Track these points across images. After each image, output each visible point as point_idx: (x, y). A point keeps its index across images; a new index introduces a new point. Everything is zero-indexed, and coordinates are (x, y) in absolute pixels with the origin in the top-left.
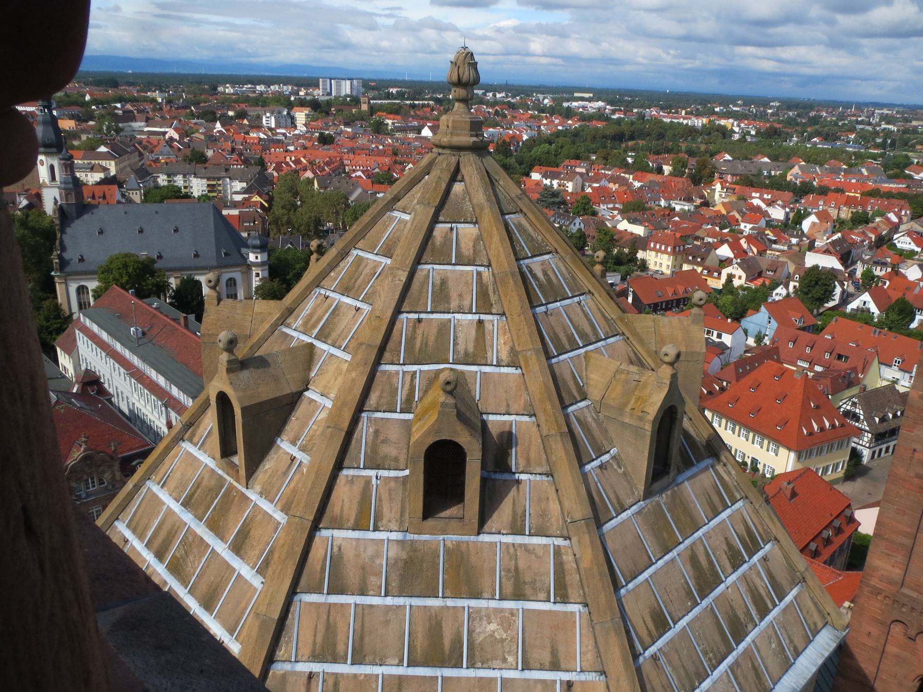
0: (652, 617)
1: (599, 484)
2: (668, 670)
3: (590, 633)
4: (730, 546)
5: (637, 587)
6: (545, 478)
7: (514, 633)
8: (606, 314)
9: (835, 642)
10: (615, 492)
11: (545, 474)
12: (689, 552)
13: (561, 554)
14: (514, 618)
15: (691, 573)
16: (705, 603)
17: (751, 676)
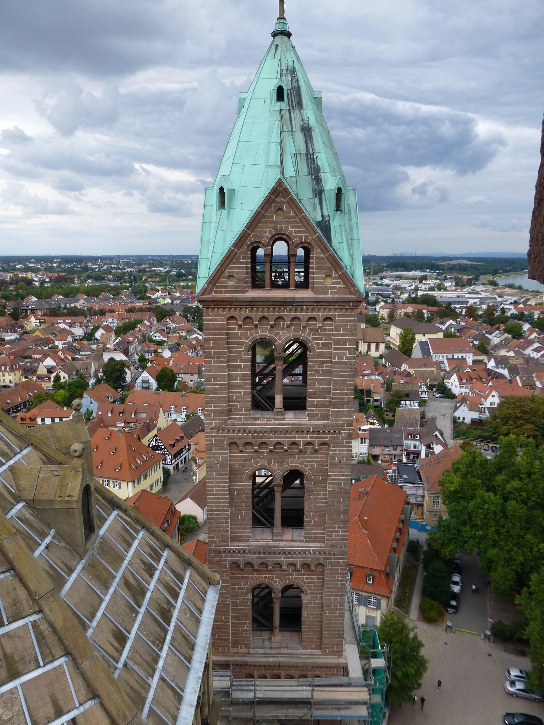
0: (115, 638)
1: (50, 561)
2: (136, 668)
3: (78, 674)
4: (144, 563)
5: (99, 622)
6: (8, 574)
7: (17, 708)
8: (16, 434)
9: (217, 593)
10: (63, 562)
11: (7, 571)
12: (123, 580)
13: (38, 626)
14: (14, 696)
15: (129, 593)
16: (142, 610)
17: (183, 642)
